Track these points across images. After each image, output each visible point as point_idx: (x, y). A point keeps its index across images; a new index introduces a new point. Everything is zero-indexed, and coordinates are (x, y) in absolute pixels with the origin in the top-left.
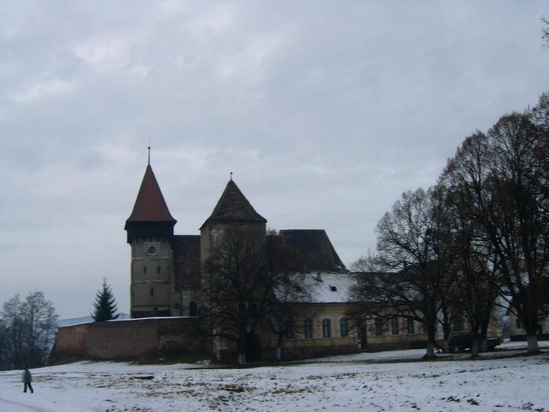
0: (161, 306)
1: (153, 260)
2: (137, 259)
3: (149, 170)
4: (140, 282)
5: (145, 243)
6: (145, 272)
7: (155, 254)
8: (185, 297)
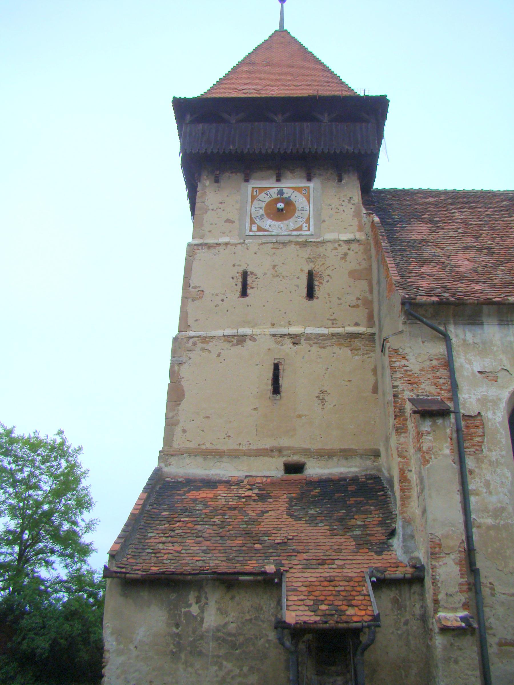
0: (327, 455)
1: (284, 244)
2: (211, 241)
4: (219, 333)
5: (254, 184)
6: (244, 293)
7: (291, 223)
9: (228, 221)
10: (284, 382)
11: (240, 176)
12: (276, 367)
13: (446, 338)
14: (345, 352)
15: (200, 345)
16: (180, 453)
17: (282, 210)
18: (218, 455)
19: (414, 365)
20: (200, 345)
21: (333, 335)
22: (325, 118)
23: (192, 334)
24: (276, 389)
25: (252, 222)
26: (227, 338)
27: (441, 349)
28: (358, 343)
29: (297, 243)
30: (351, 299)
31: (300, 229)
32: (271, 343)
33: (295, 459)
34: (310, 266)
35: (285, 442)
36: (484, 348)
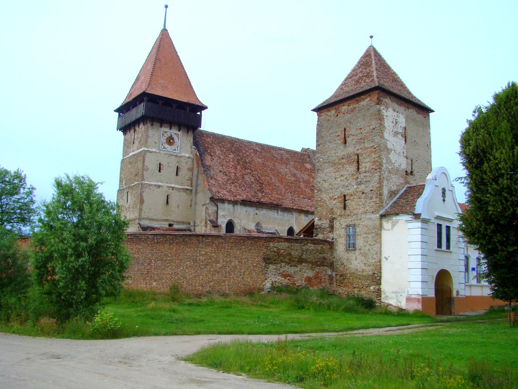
0: (178, 223)
1: (171, 155)
2: (151, 150)
3: (164, 33)
5: (164, 129)
6: (160, 171)
7: (173, 147)
8: (221, 213)
9: (155, 142)
10: (169, 201)
11: (158, 125)
12: (168, 196)
13: (217, 206)
14: (184, 194)
15: (148, 187)
16: (144, 219)
17: (170, 141)
18: (153, 220)
19: (210, 211)
20: (148, 187)
21: (182, 189)
22: (188, 109)
23: (146, 182)
24: (167, 203)
25: (162, 145)
26: (155, 185)
27: (215, 208)
28: (188, 192)
29: (175, 156)
30: (187, 178)
31: (175, 150)
32: (166, 189)
33: (171, 223)
34: (177, 165)
35: (168, 218)
36: (224, 209)
